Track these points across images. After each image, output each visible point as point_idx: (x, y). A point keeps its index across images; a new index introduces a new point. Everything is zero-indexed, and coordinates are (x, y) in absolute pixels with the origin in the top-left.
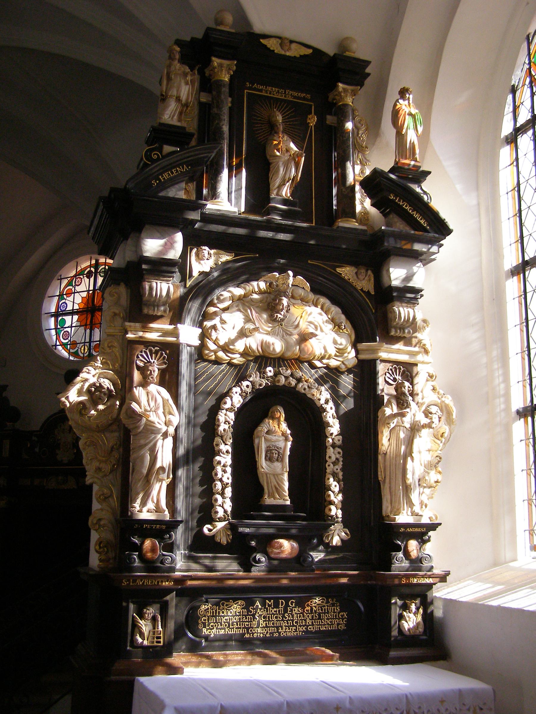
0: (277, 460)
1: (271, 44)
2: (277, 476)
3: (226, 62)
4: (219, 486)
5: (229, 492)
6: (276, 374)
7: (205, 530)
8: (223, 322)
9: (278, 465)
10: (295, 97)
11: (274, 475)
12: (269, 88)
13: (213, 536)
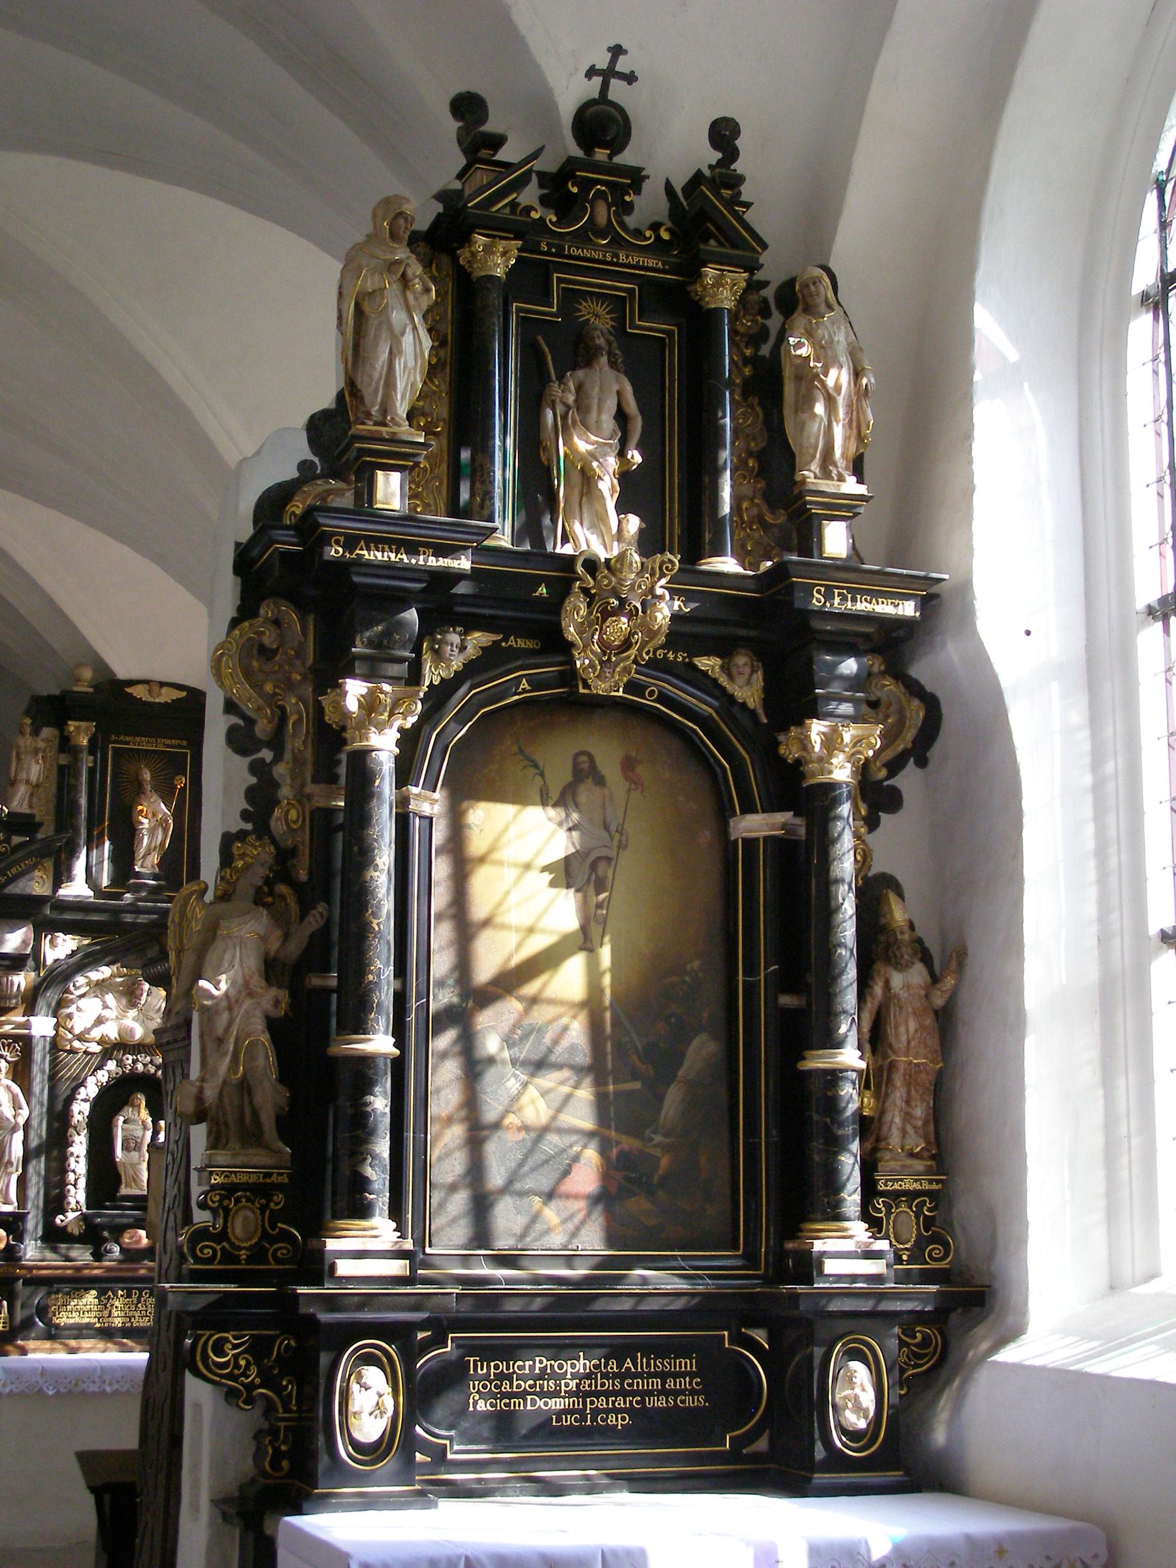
0: (135, 1149)
1: (139, 692)
2: (135, 1166)
3: (83, 724)
4: (71, 1177)
5: (82, 1183)
6: (134, 1062)
7: (58, 1221)
8: (79, 1009)
9: (135, 1154)
10: (168, 746)
11: (131, 1165)
12: (138, 739)
13: (66, 1227)
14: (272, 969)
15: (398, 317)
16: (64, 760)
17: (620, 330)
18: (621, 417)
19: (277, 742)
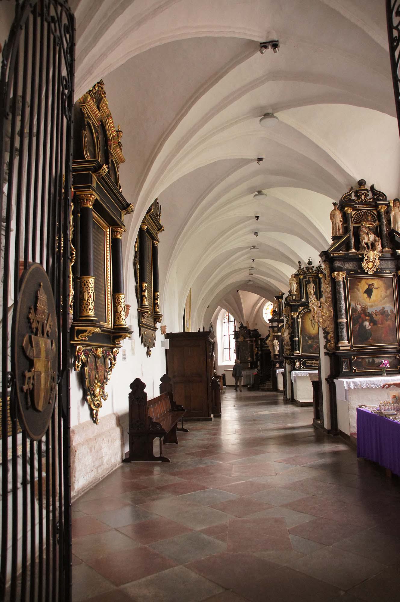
14: (289, 334)
15: (294, 284)
16: (279, 303)
17: (313, 280)
18: (313, 287)
19: (288, 317)
